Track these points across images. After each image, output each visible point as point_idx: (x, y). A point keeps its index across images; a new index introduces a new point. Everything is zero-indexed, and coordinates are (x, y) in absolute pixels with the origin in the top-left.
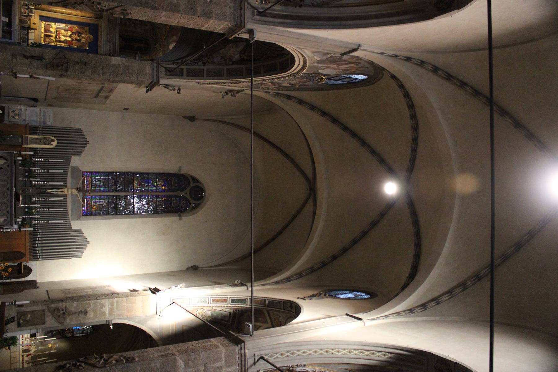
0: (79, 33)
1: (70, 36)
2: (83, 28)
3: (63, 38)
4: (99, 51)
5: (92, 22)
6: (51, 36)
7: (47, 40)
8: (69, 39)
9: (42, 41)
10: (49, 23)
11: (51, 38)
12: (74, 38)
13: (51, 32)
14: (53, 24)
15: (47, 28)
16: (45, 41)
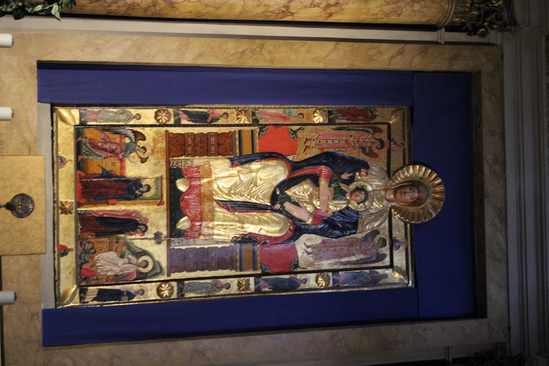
0: (339, 167)
1: (278, 197)
2: (367, 121)
3: (223, 230)
4: (494, 291)
5: (435, 62)
6: (132, 224)
7: (108, 262)
8: (268, 227)
9: (69, 285)
10: (109, 115)
11: (138, 241)
12: (304, 214)
13: (131, 189)
14: (148, 115)
15: (98, 164)
16: (84, 278)
